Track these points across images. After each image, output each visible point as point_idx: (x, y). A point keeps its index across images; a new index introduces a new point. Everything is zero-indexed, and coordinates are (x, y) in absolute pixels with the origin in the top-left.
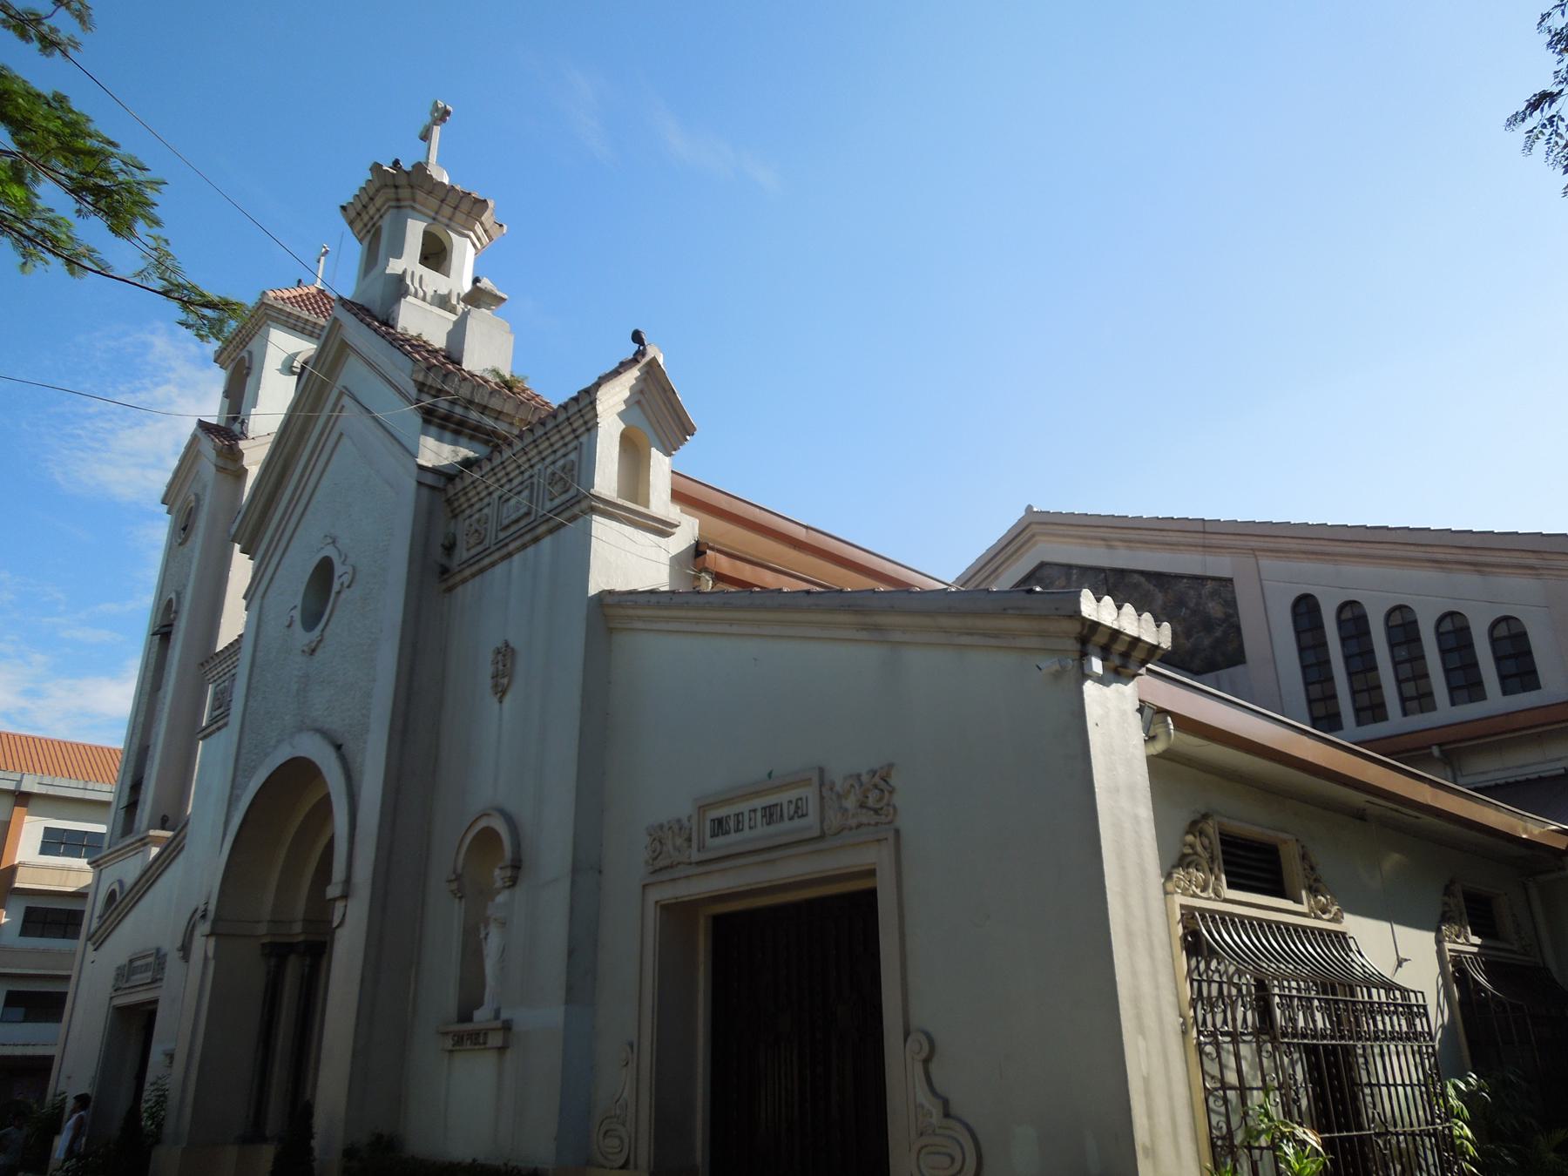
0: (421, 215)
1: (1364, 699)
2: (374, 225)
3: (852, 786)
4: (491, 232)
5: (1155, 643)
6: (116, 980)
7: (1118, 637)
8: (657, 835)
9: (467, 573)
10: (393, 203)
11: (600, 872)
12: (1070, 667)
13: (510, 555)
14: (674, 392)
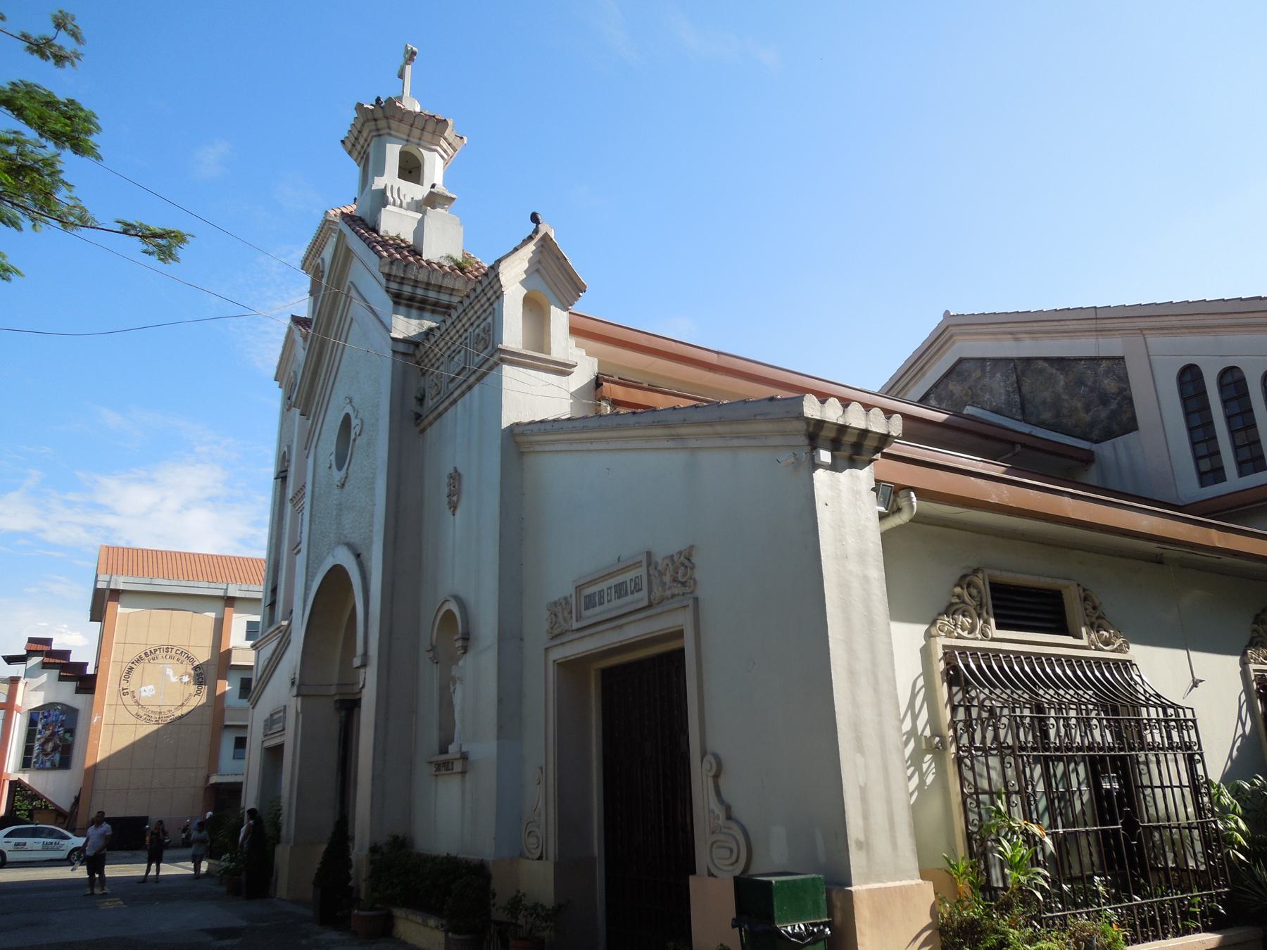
0: (397, 139)
1: (1246, 454)
2: (365, 152)
3: (667, 565)
4: (454, 144)
6: (265, 728)
8: (558, 609)
9: (431, 417)
10: (375, 133)
11: (522, 640)
12: (803, 460)
13: (455, 401)
14: (566, 259)
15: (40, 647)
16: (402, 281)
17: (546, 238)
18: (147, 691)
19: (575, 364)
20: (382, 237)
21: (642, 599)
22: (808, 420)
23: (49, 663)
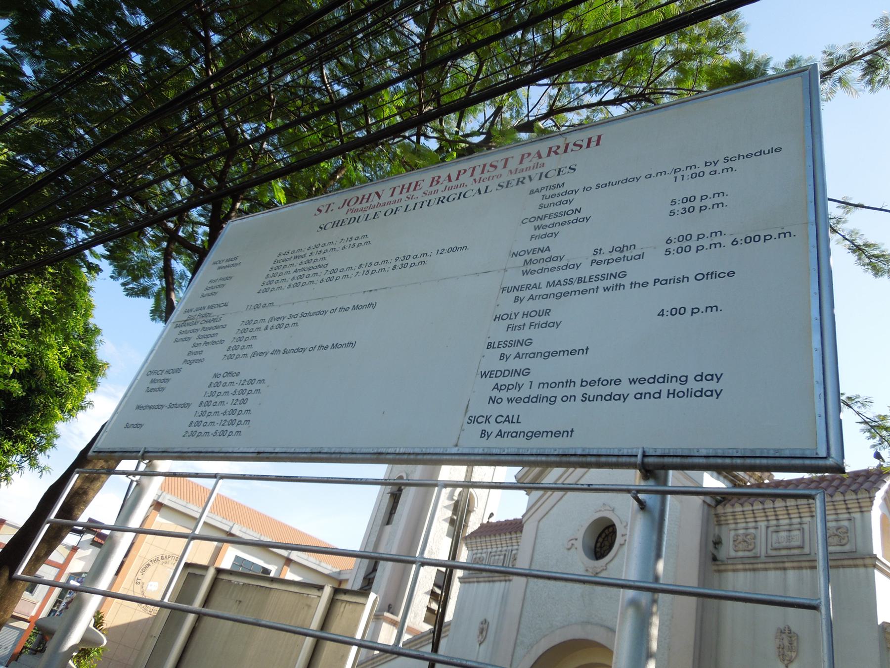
23: (97, 542)
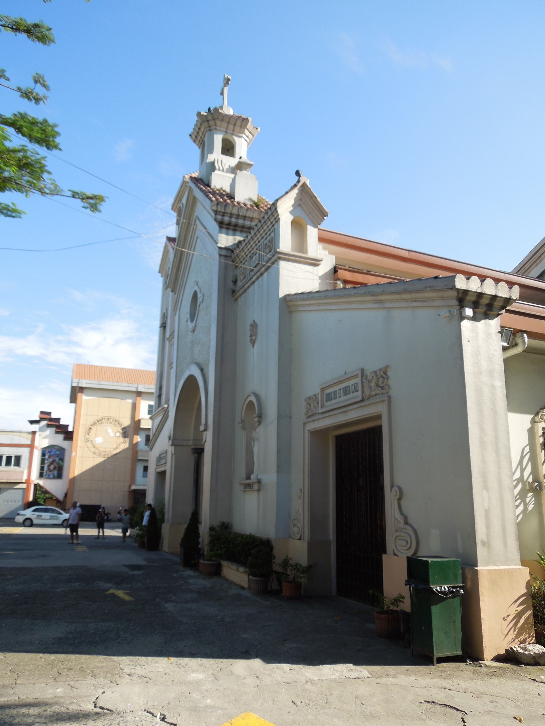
3: (373, 376)
4: (252, 132)
5: (508, 297)
6: (157, 462)
7: (482, 296)
8: (311, 400)
9: (241, 292)
10: (207, 129)
11: (291, 418)
12: (455, 314)
13: (254, 282)
14: (316, 197)
15: (45, 416)
16: (223, 214)
17: (304, 185)
18: (99, 440)
19: (321, 259)
20: (213, 189)
21: (358, 396)
22: (458, 290)
